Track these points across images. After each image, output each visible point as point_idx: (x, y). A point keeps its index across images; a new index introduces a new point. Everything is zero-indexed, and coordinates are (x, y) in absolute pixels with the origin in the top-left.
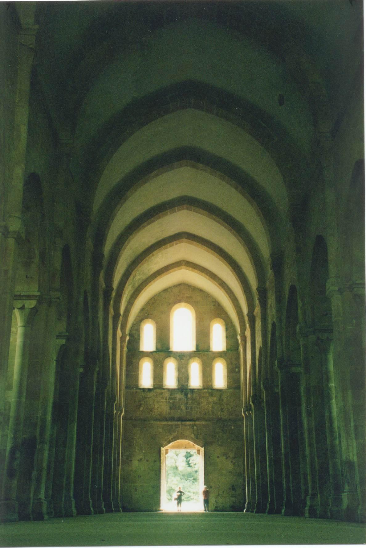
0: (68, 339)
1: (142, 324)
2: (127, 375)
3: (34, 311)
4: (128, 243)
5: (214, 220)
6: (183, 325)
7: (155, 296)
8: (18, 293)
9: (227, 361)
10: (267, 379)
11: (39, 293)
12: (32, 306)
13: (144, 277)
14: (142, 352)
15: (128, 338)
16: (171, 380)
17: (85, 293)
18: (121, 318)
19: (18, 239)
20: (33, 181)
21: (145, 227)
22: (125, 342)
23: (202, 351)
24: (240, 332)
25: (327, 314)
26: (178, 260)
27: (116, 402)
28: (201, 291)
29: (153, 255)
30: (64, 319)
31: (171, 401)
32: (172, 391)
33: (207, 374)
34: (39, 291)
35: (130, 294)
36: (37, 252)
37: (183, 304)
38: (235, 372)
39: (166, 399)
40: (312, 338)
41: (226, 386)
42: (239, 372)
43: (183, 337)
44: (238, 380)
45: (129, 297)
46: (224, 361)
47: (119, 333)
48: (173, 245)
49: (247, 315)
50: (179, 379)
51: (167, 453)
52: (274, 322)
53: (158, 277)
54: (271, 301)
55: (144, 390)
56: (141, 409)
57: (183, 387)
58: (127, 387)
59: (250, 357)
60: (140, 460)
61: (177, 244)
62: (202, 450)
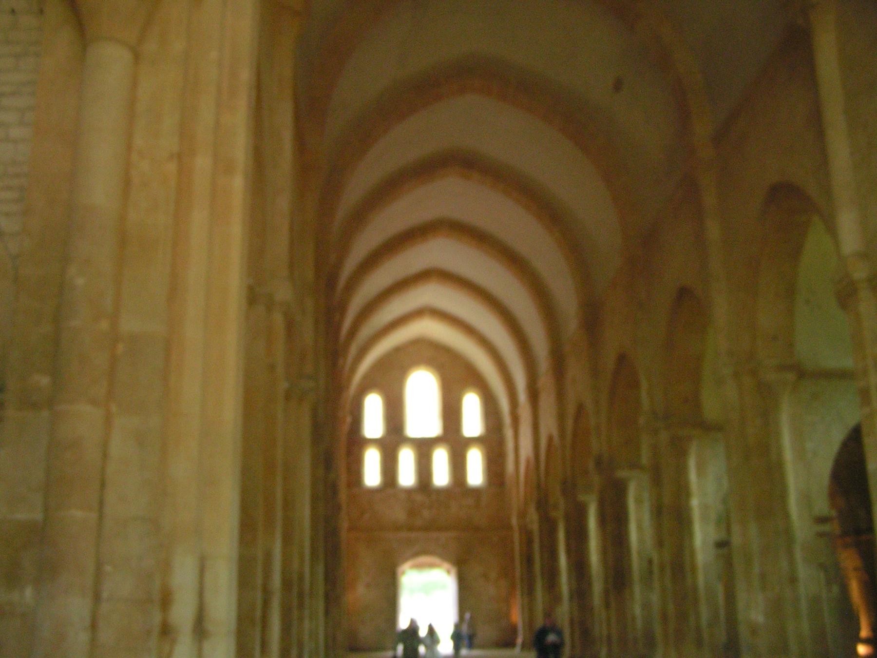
16: (407, 477)
23: (452, 436)
32: (408, 491)
40: (664, 436)
51: (403, 573)
54: (576, 370)
60: (368, 586)
62: (454, 571)
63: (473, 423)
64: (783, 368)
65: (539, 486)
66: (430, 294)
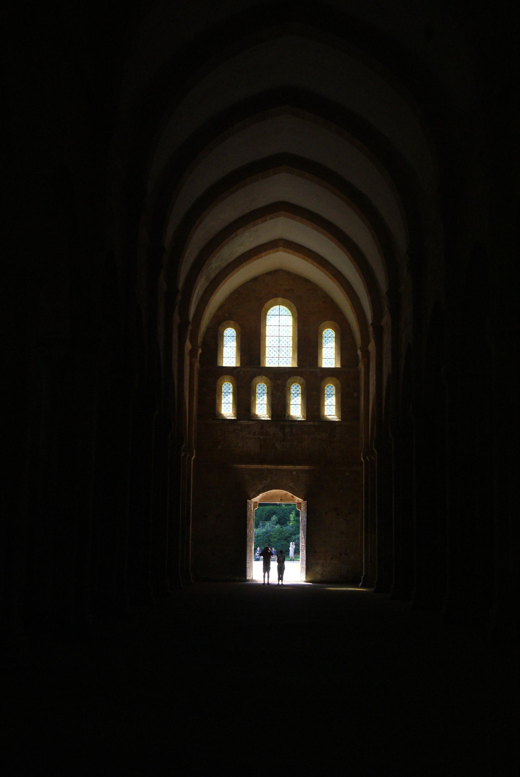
7: (240, 287)
13: (224, 265)
14: (223, 367)
15: (200, 351)
16: (262, 409)
18: (190, 327)
22: (196, 357)
26: (272, 239)
27: (184, 446)
28: (306, 281)
29: (237, 235)
31: (262, 437)
33: (313, 403)
37: (280, 299)
39: (254, 434)
42: (358, 397)
45: (201, 293)
46: (338, 382)
47: (188, 345)
48: (266, 221)
49: (372, 324)
56: (220, 447)
59: (375, 377)
61: (271, 219)
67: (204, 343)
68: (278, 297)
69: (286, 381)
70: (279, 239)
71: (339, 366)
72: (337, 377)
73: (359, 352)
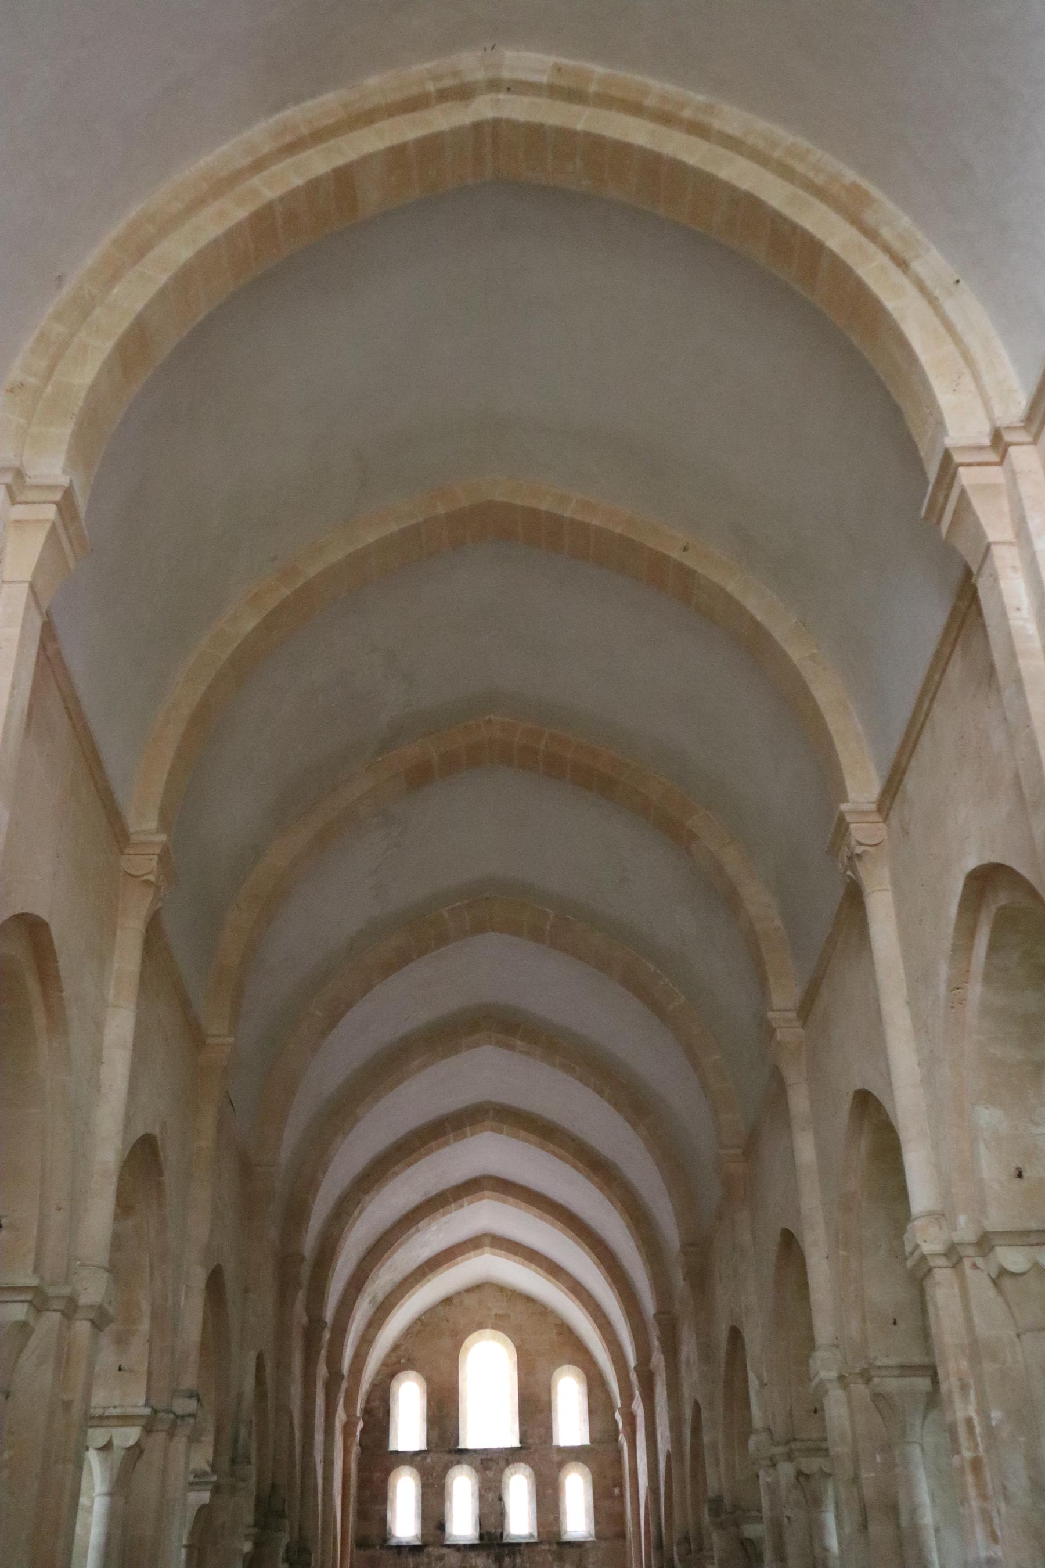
0: (216, 1490)
1: (394, 1384)
2: (363, 1515)
3: (136, 1451)
4: (361, 1212)
5: (554, 1153)
6: (488, 1377)
8: (99, 1412)
9: (593, 1473)
10: (686, 1539)
11: (147, 1411)
12: (131, 1442)
14: (397, 1452)
15: (361, 1425)
16: (462, 1524)
17: (260, 1358)
18: (344, 1385)
19: (100, 1321)
20: (143, 1158)
21: (397, 1174)
24: (619, 1405)
25: (815, 1411)
28: (529, 1300)
29: (418, 1231)
30: (209, 1439)
34: (146, 1404)
35: (366, 1320)
36: (145, 1306)
37: (488, 1332)
38: (611, 1496)
40: (786, 1470)
41: (593, 1532)
42: (622, 1495)
43: (489, 1418)
44: (621, 1517)
47: (341, 1416)
48: (462, 1206)
50: (481, 1522)
52: (696, 1403)
53: (430, 1276)
54: (689, 1349)
55: (400, 1549)
57: (491, 1537)
58: (362, 1543)
61: (471, 1203)
63: (571, 1424)
64: (906, 1370)
65: (660, 1546)
66: (487, 1214)
67: (367, 1411)
68: (485, 1328)
69: (502, 1471)
70: (485, 1235)
71: (586, 1441)
72: (585, 1462)
73: (618, 1417)
